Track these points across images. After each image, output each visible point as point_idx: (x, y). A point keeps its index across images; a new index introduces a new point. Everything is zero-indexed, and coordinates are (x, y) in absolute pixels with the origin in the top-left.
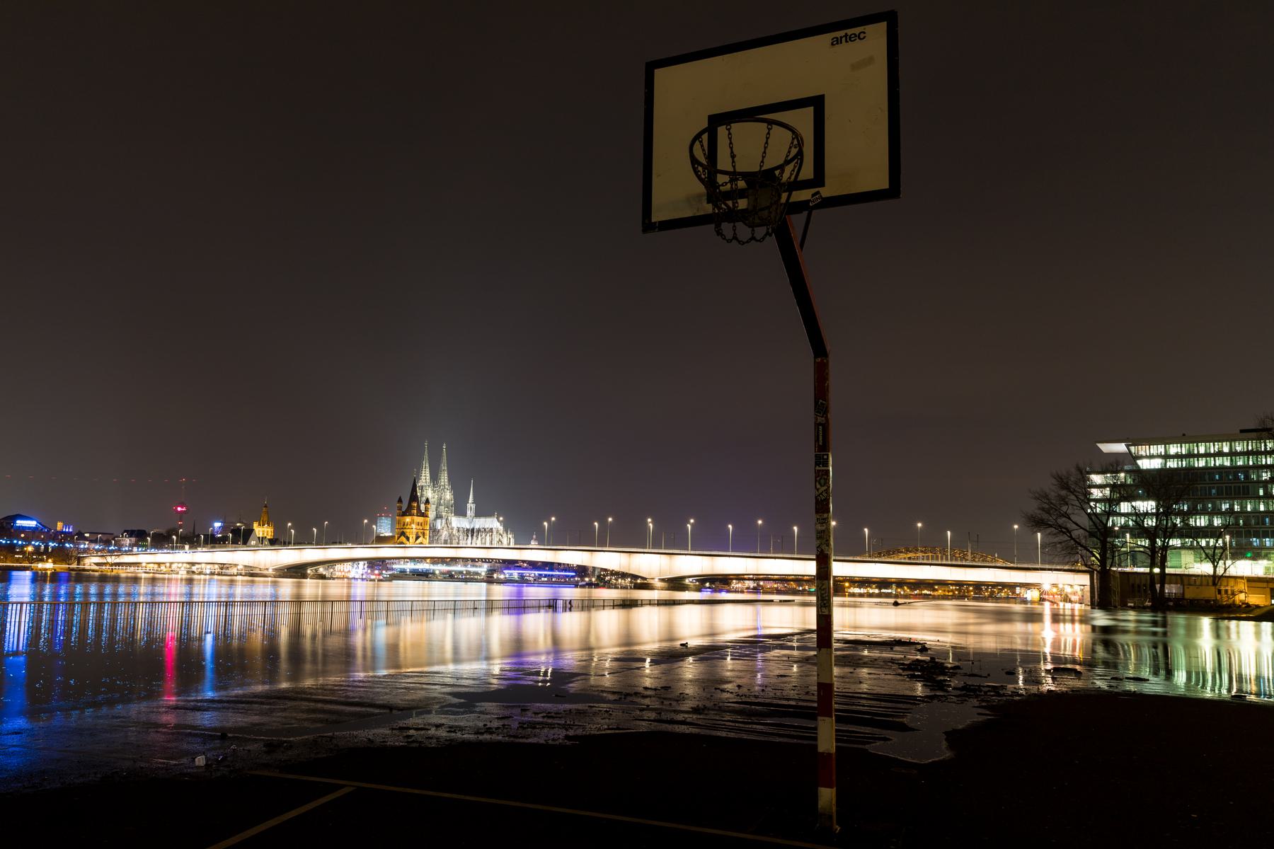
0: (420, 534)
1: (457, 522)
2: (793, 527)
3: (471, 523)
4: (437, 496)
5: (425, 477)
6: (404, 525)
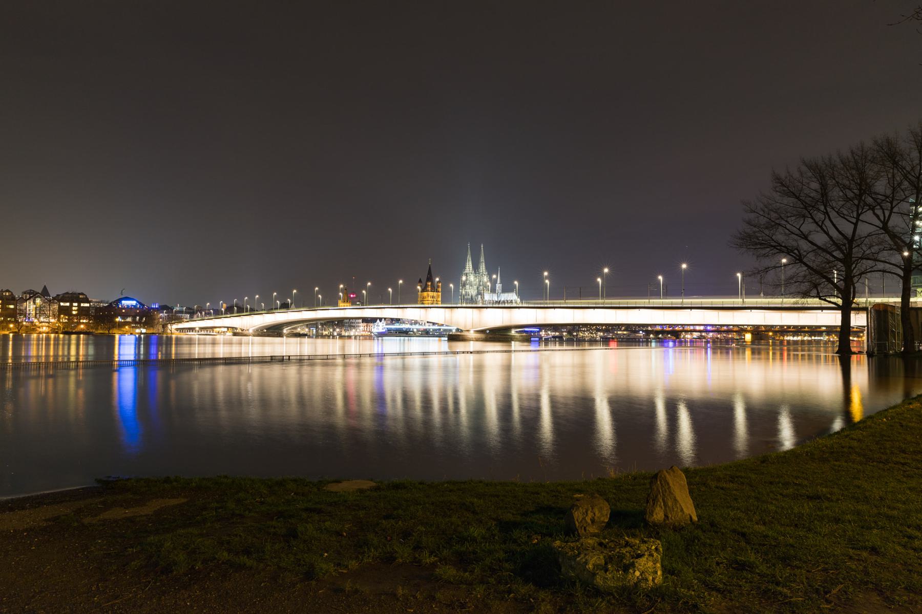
2: (596, 279)
4: (477, 280)
5: (469, 266)
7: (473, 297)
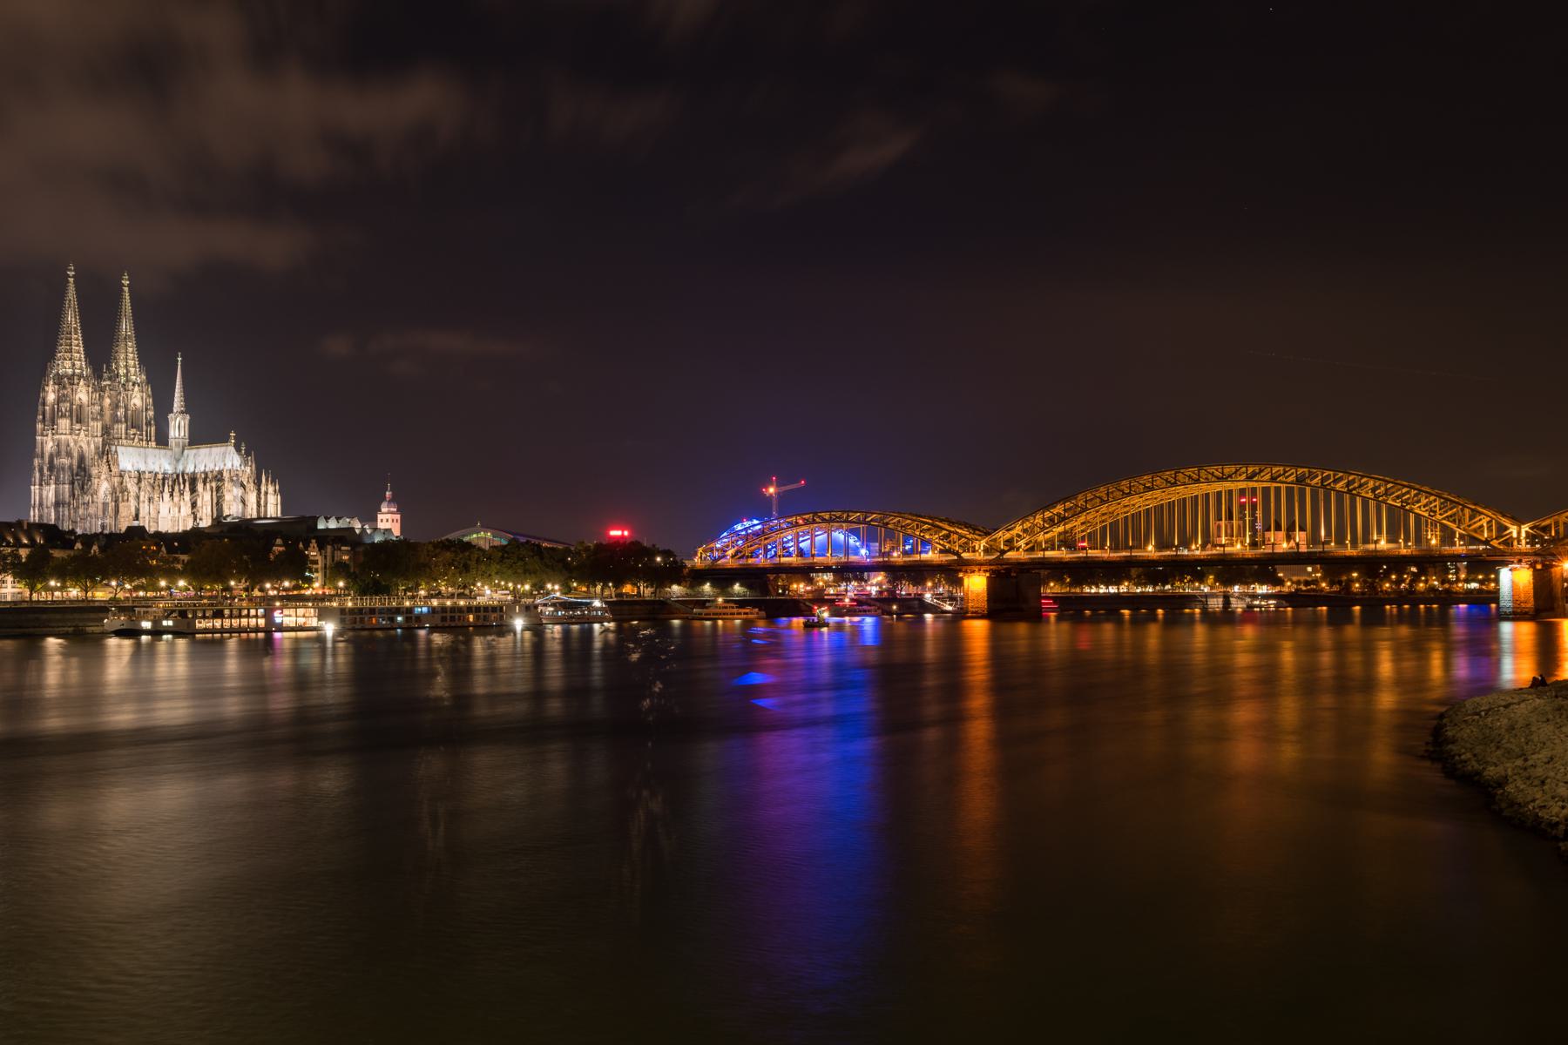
1: (130, 459)
3: (178, 461)
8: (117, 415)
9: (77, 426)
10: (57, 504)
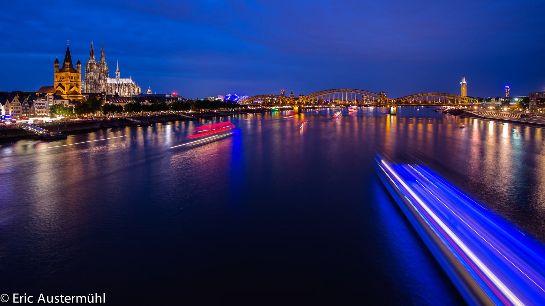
0: (74, 85)
1: (109, 81)
3: (118, 81)
6: (61, 78)
7: (96, 81)
8: (101, 71)
9: (94, 74)
10: (91, 89)
